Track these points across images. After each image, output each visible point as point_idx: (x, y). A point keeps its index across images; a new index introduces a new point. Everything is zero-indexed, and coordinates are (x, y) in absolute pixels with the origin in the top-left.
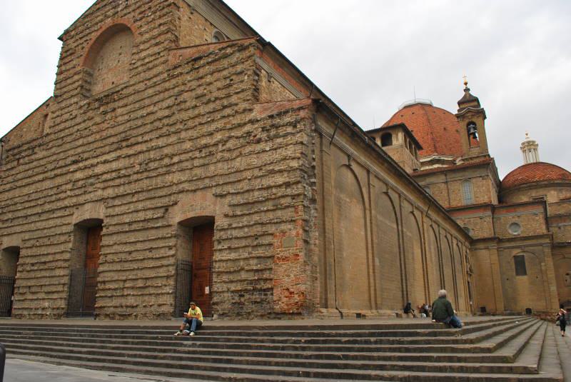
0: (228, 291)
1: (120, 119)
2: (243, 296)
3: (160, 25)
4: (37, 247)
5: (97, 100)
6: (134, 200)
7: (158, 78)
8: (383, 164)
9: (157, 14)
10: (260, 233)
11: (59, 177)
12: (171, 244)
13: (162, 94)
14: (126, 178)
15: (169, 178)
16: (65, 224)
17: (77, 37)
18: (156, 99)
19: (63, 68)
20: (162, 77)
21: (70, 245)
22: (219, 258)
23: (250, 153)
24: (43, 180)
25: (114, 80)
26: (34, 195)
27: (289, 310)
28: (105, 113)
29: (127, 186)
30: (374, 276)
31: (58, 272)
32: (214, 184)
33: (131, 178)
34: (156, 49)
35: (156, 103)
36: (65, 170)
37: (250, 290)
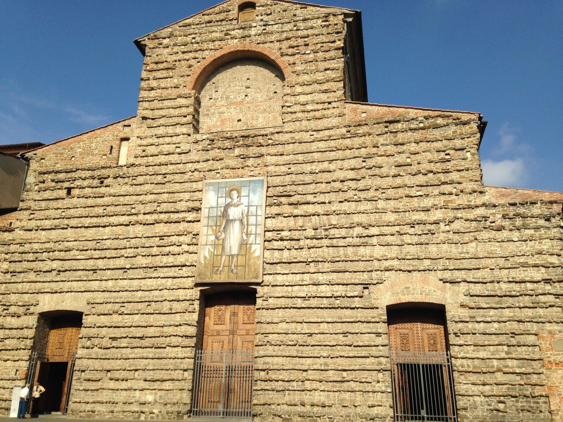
1: (272, 169)
2: (504, 403)
3: (326, 70)
5: (228, 138)
7: (331, 132)
9: (318, 55)
11: (162, 224)
12: (380, 331)
17: (176, 49)
19: (154, 84)
20: (338, 131)
22: (462, 355)
25: (241, 118)
26: (108, 243)
28: (245, 157)
32: (440, 268)
33: (302, 243)
35: (333, 160)
36: (174, 217)
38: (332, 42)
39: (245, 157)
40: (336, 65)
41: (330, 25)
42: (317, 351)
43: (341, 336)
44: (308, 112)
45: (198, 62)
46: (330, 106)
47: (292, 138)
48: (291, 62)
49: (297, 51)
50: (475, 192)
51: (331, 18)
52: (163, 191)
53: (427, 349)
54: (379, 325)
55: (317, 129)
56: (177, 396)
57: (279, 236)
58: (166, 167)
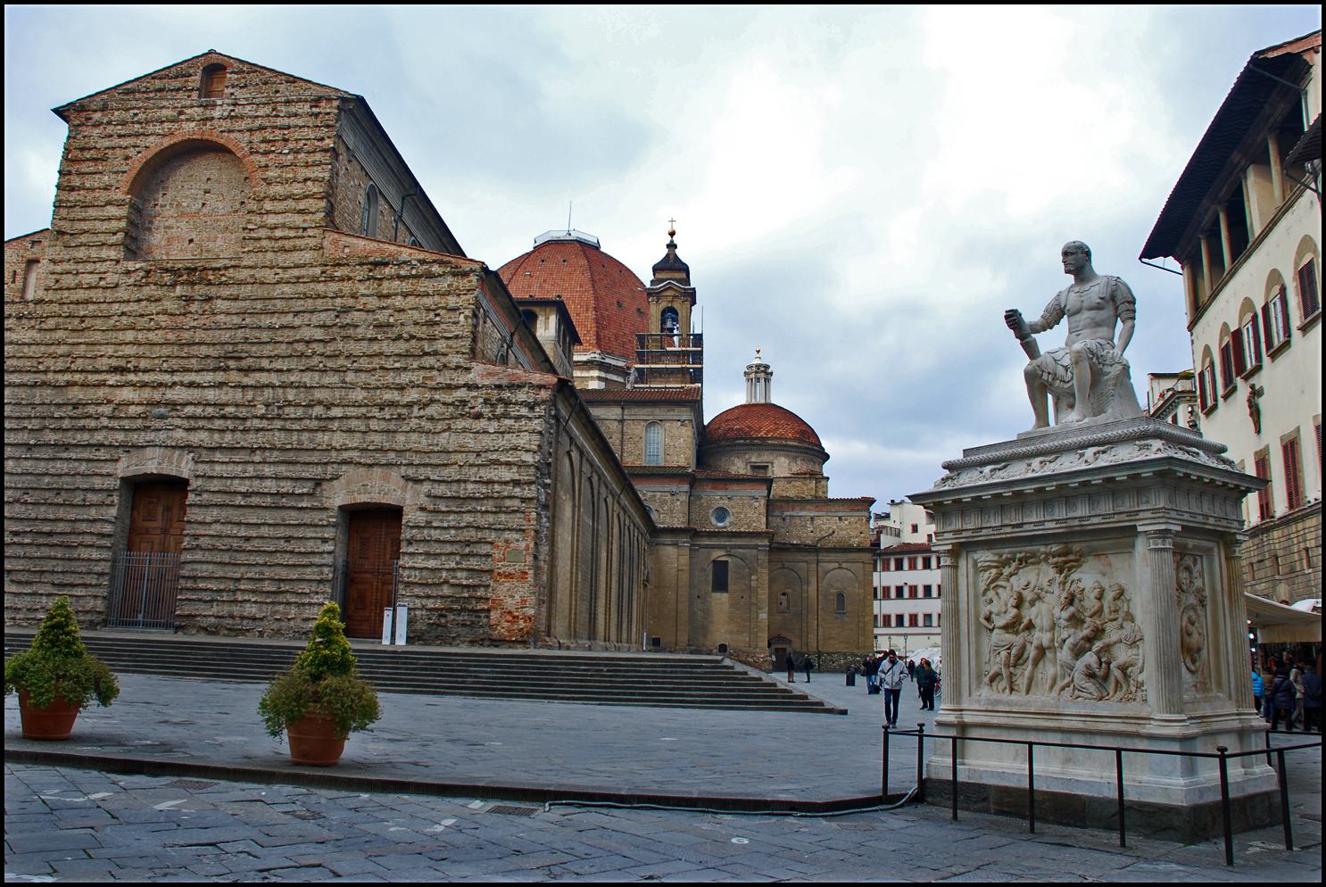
0: (421, 609)
2: (445, 616)
3: (306, 180)
4: (26, 503)
5: (167, 270)
6: (257, 458)
7: (303, 272)
8: (593, 439)
9: (299, 157)
10: (475, 539)
11: (76, 388)
12: (326, 536)
13: (310, 301)
14: (238, 422)
15: (323, 438)
16: (102, 475)
17: (110, 129)
18: (298, 305)
19: (76, 181)
21: (113, 511)
22: (410, 564)
23: (464, 430)
24: (35, 385)
25: (194, 236)
27: (511, 636)
28: (189, 300)
29: (238, 435)
30: (576, 595)
31: (84, 553)
32: (404, 462)
33: (248, 424)
34: (298, 220)
36: (93, 378)
37: (457, 610)
38: (318, 140)
39: (189, 300)
40: (320, 175)
41: (320, 113)
42: (253, 559)
43: (282, 541)
44: (277, 239)
45: (139, 152)
46: (305, 234)
47: (252, 276)
48: (263, 164)
49: (273, 149)
50: (457, 367)
51: (323, 104)
52: (80, 341)
53: (388, 556)
54: (327, 529)
55: (285, 265)
56: (91, 604)
57: (222, 412)
58: (85, 306)
